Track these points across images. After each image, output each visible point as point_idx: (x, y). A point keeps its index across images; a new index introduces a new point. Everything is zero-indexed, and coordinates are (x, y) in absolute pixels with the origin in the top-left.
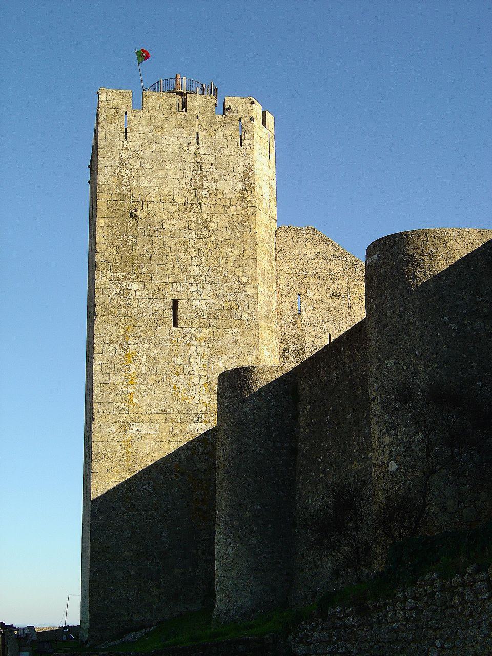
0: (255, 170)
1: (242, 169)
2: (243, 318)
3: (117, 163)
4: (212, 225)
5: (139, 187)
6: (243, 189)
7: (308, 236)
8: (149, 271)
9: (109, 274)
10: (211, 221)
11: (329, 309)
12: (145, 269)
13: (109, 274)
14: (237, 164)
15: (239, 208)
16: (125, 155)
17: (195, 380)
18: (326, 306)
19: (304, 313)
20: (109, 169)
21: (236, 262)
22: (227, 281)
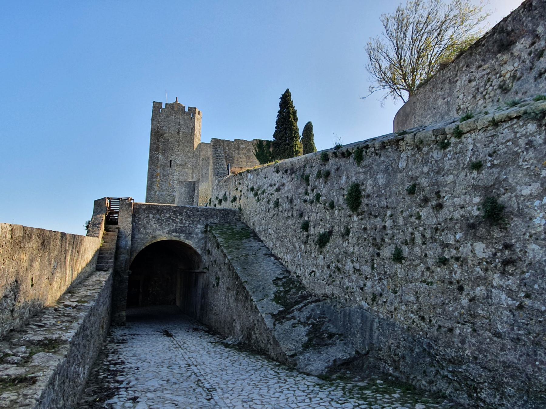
22: (185, 156)
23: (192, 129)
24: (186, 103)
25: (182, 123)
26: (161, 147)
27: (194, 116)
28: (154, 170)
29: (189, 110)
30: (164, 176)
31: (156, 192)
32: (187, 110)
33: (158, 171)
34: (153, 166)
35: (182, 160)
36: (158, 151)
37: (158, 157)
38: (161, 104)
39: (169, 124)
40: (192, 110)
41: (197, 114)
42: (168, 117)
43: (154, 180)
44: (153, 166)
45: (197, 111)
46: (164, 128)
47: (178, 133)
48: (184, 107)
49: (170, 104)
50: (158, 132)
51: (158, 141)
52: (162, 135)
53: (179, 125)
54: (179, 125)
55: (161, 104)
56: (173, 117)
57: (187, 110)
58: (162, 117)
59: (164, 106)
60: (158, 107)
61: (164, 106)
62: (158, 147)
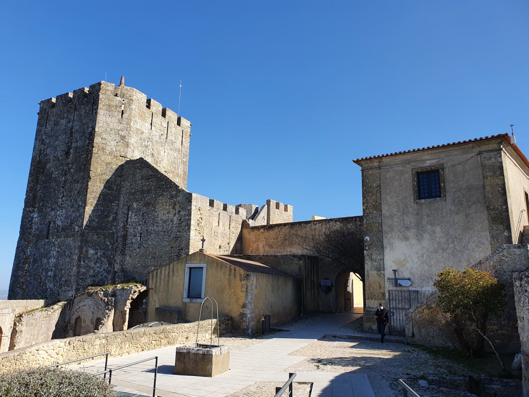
0: (96, 130)
2: (76, 230)
4: (72, 170)
5: (46, 155)
6: (88, 143)
7: (138, 165)
8: (42, 205)
10: (72, 168)
11: (143, 214)
14: (88, 128)
15: (85, 156)
16: (44, 137)
17: (49, 273)
18: (141, 213)
19: (129, 220)
21: (78, 192)
22: (72, 206)
26: (39, 194)
35: (67, 218)
47: (67, 153)
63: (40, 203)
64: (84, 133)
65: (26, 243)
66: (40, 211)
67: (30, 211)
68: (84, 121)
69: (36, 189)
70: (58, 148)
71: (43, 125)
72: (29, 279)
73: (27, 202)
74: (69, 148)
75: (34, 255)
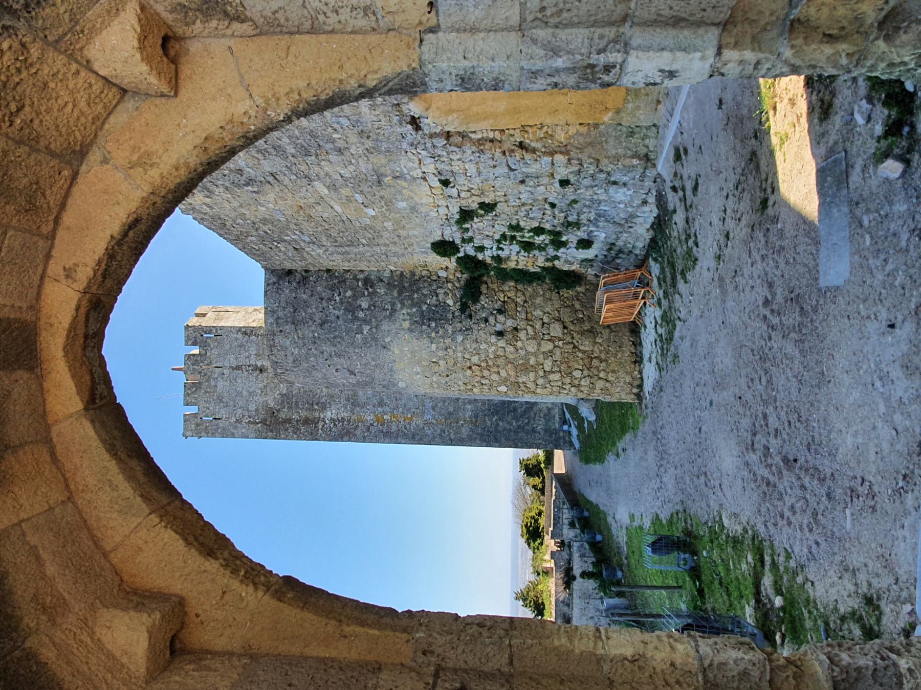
1: (240, 336)
3: (239, 425)
5: (257, 410)
8: (317, 404)
9: (320, 431)
12: (316, 407)
13: (320, 431)
14: (236, 339)
16: (233, 419)
20: (244, 430)
23: (245, 333)
24: (182, 350)
25: (232, 360)
26: (304, 414)
27: (209, 330)
28: (368, 429)
29: (195, 344)
30: (381, 404)
31: (426, 423)
32: (196, 351)
33: (370, 418)
34: (358, 432)
36: (315, 421)
37: (332, 420)
38: (187, 419)
39: (240, 394)
40: (196, 336)
41: (204, 322)
42: (220, 399)
43: (394, 428)
44: (358, 432)
45: (194, 321)
46: (252, 407)
48: (189, 357)
49: (187, 395)
50: (263, 422)
51: (289, 421)
52: (272, 413)
53: (238, 368)
54: (238, 368)
55: (187, 419)
56: (221, 384)
57: (196, 351)
58: (223, 413)
59: (193, 410)
60: (198, 425)
61: (193, 410)
62: (306, 421)
63: (315, 410)
64: (240, 346)
65: (360, 424)
66: (324, 407)
67: (323, 426)
68: (227, 347)
69: (298, 421)
70: (251, 390)
71: (217, 425)
72: (400, 410)
73: (313, 436)
74: (256, 368)
75: (374, 406)
